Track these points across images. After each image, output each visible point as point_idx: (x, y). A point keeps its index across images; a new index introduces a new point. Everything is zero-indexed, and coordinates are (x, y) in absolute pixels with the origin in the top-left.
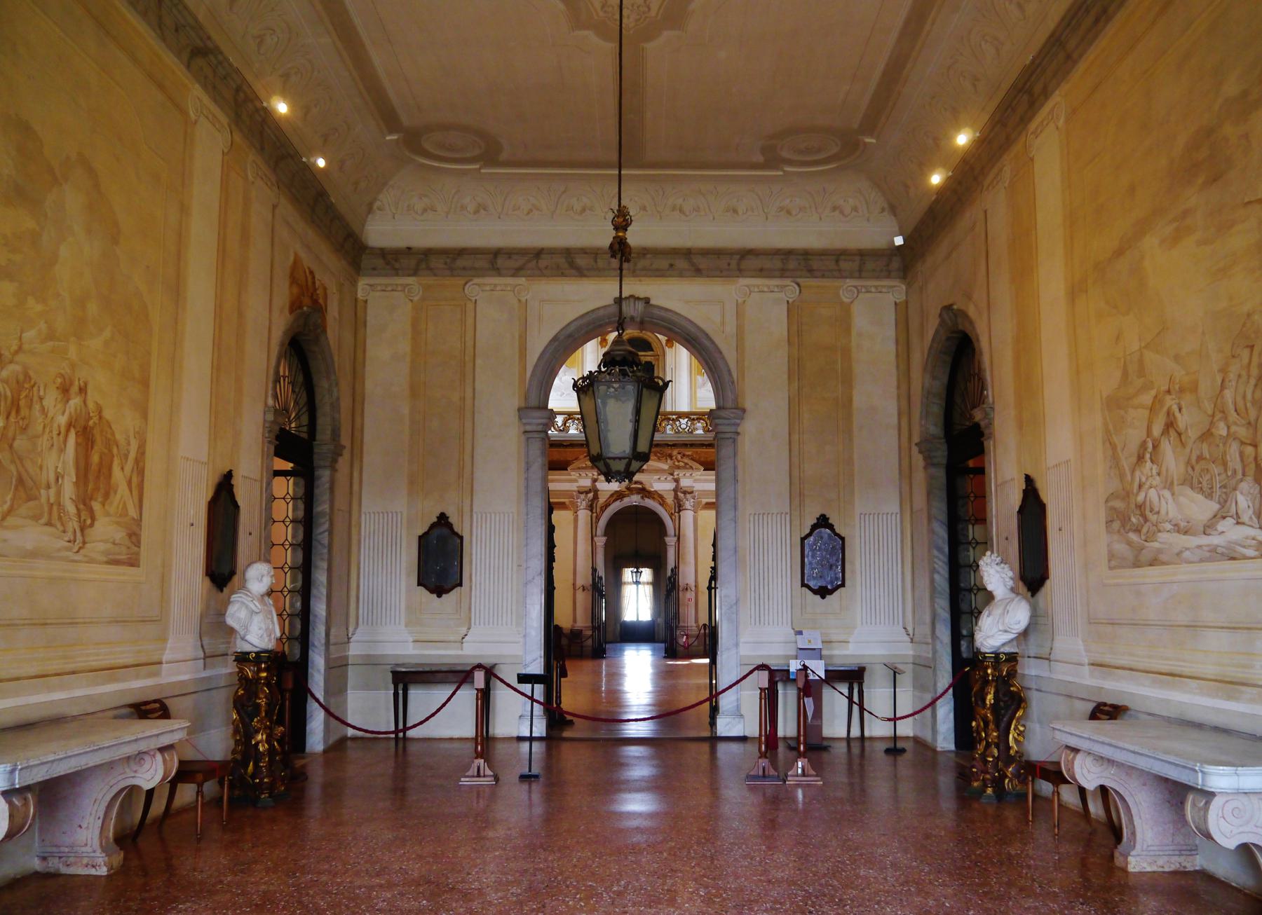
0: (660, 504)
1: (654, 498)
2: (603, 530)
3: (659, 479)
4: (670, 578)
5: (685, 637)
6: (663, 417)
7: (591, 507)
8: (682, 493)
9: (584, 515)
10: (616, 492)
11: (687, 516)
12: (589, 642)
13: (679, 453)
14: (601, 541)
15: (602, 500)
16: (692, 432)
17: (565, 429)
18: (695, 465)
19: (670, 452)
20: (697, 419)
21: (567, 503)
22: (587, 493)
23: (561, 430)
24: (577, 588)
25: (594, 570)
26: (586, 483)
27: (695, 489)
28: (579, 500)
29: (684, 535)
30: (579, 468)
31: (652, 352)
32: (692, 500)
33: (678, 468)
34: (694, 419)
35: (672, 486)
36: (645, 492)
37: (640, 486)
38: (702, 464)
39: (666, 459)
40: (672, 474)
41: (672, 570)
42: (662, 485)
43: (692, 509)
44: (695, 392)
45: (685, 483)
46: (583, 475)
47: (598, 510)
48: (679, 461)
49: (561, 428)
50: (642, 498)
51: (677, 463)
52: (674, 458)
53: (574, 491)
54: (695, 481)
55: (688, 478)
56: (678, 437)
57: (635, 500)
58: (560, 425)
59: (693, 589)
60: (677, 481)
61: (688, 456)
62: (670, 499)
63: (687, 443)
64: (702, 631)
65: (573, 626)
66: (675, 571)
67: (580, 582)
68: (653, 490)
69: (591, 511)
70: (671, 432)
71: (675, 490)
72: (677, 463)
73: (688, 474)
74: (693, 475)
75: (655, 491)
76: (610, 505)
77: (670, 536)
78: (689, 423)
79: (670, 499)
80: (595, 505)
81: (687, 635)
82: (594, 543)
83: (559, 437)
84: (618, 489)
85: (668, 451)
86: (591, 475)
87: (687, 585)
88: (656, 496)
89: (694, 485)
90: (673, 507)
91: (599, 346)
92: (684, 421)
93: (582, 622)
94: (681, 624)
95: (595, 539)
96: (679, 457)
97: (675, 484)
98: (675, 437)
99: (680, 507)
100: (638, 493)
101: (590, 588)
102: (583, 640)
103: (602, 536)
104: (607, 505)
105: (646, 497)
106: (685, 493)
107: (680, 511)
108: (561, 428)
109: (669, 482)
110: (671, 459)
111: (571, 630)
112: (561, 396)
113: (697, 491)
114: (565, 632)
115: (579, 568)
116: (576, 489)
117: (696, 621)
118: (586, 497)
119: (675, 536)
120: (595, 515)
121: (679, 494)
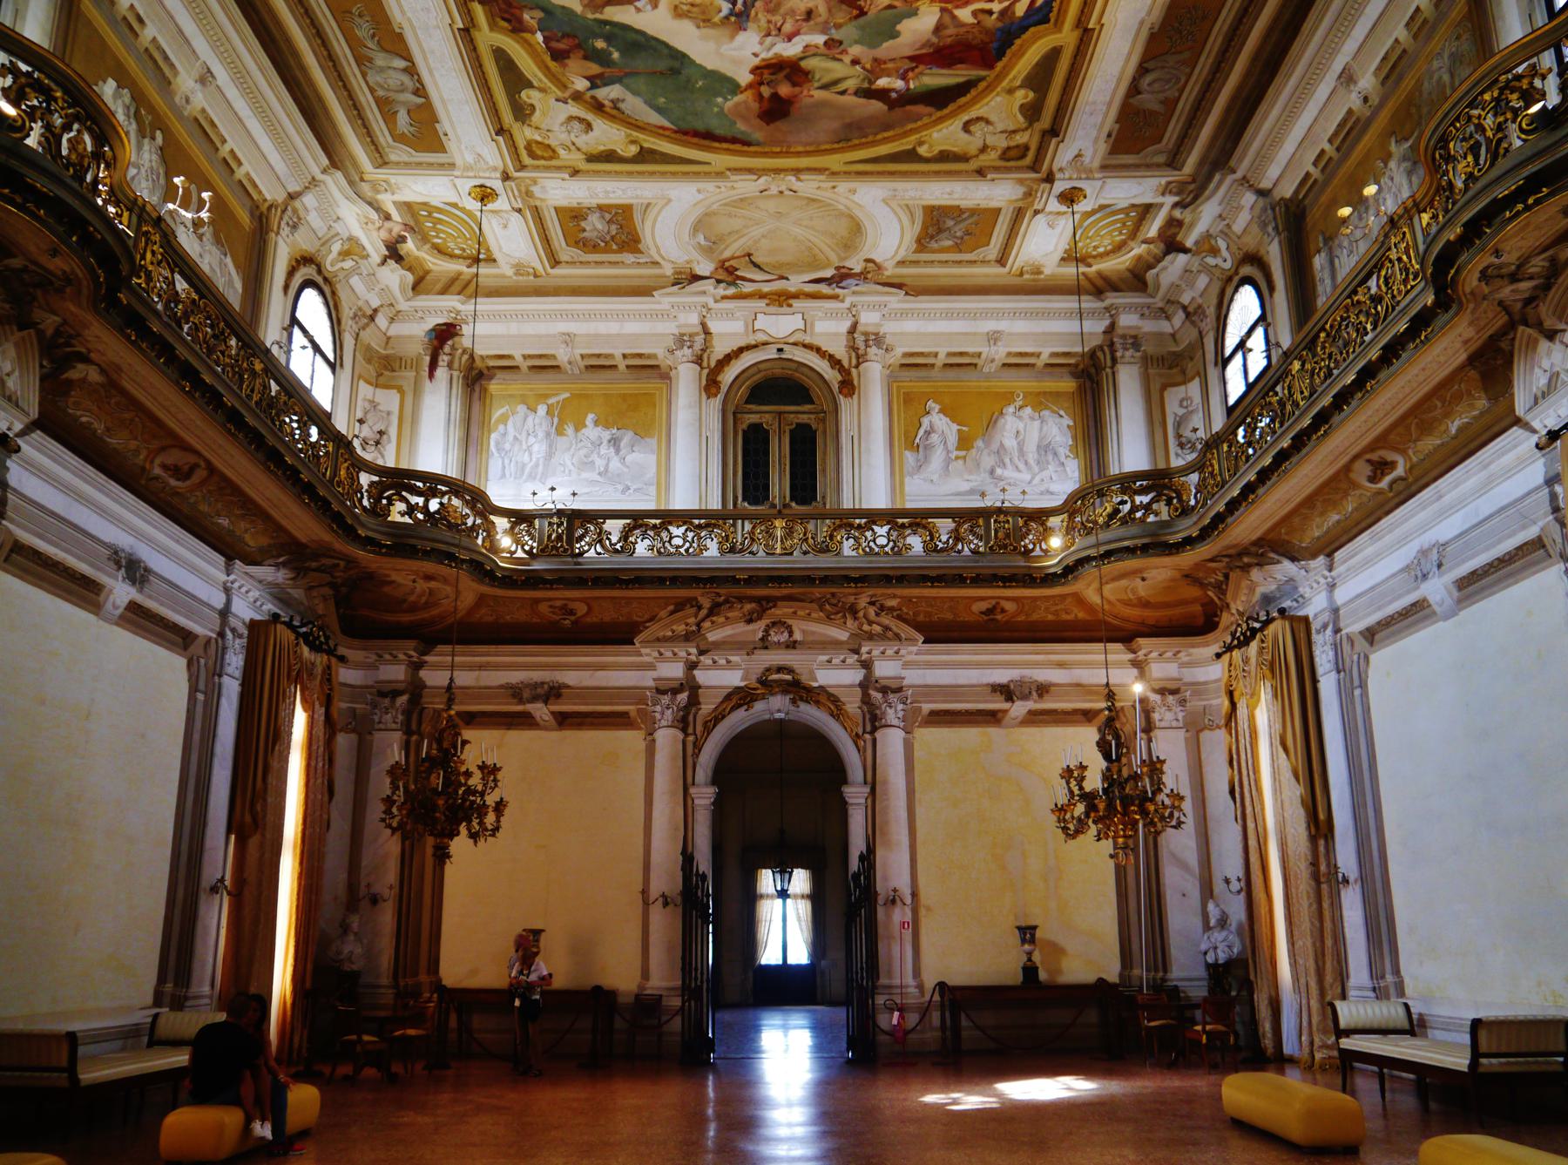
0: (832, 715)
1: (817, 703)
2: (710, 773)
3: (829, 661)
4: (856, 876)
5: (896, 1014)
6: (838, 522)
7: (683, 723)
8: (878, 690)
9: (667, 739)
10: (738, 690)
11: (892, 741)
12: (676, 1024)
13: (872, 603)
14: (704, 796)
15: (707, 707)
16: (899, 553)
17: (627, 548)
18: (906, 630)
19: (852, 599)
20: (911, 525)
21: (633, 714)
22: (675, 691)
23: (616, 551)
24: (652, 899)
25: (688, 858)
26: (673, 670)
27: (905, 682)
28: (658, 708)
29: (885, 782)
30: (658, 640)
31: (807, 407)
32: (900, 707)
33: (871, 637)
34: (903, 526)
35: (855, 676)
36: (799, 690)
37: (788, 677)
38: (918, 627)
39: (845, 617)
40: (856, 652)
41: (862, 858)
42: (838, 676)
43: (902, 725)
44: (902, 484)
45: (885, 669)
46: (668, 654)
47: (699, 728)
48: (870, 623)
49: (618, 547)
50: (794, 701)
51: (866, 627)
52: (861, 614)
53: (646, 688)
54: (906, 665)
55: (890, 658)
56: (871, 562)
57: (776, 706)
58: (614, 539)
59: (908, 900)
60: (867, 665)
61: (891, 609)
62: (853, 705)
63: (891, 573)
64: (937, 997)
65: (642, 987)
66: (868, 858)
67: (656, 888)
68: (815, 684)
69: (684, 730)
70: (854, 553)
71: (865, 685)
72: (866, 627)
73: (890, 652)
74: (902, 652)
75: (821, 687)
76: (724, 717)
77: (853, 785)
78: (895, 534)
79: (853, 705)
80: (691, 718)
81: (901, 1009)
82: (690, 802)
83: (611, 562)
84: (742, 684)
85: (846, 593)
86: (683, 654)
87: (895, 890)
88: (823, 699)
89: (904, 673)
90: (860, 721)
91: (704, 396)
92: (881, 530)
93: (662, 978)
94: (883, 981)
95: (692, 790)
96: (872, 611)
97: (864, 671)
98: (862, 562)
99: (874, 721)
100: (785, 692)
101: (679, 900)
102: (664, 1018)
103: (706, 785)
104: (717, 718)
105: (801, 699)
106: (885, 690)
107: (874, 729)
108: (618, 547)
109: (851, 667)
110: (856, 619)
111: (637, 996)
112: (623, 492)
113: (910, 686)
114: (621, 1000)
115: (656, 858)
116: (651, 683)
117: (917, 973)
118: (673, 700)
119: (865, 783)
120: (691, 738)
121: (873, 693)
